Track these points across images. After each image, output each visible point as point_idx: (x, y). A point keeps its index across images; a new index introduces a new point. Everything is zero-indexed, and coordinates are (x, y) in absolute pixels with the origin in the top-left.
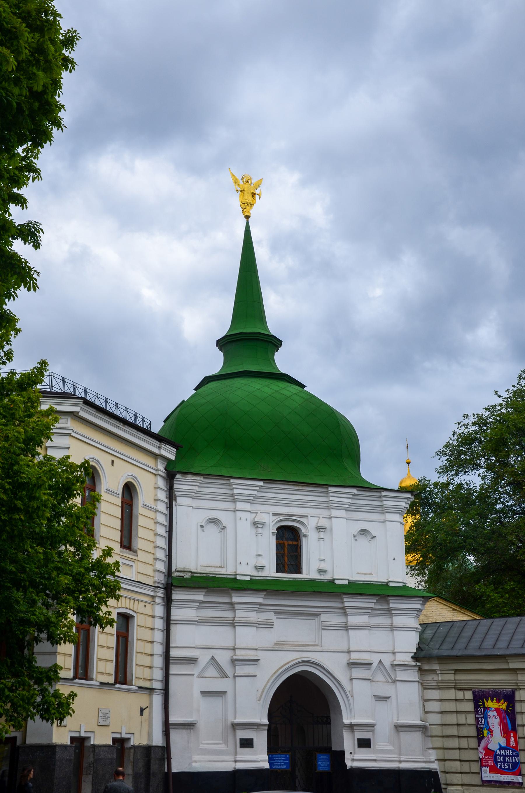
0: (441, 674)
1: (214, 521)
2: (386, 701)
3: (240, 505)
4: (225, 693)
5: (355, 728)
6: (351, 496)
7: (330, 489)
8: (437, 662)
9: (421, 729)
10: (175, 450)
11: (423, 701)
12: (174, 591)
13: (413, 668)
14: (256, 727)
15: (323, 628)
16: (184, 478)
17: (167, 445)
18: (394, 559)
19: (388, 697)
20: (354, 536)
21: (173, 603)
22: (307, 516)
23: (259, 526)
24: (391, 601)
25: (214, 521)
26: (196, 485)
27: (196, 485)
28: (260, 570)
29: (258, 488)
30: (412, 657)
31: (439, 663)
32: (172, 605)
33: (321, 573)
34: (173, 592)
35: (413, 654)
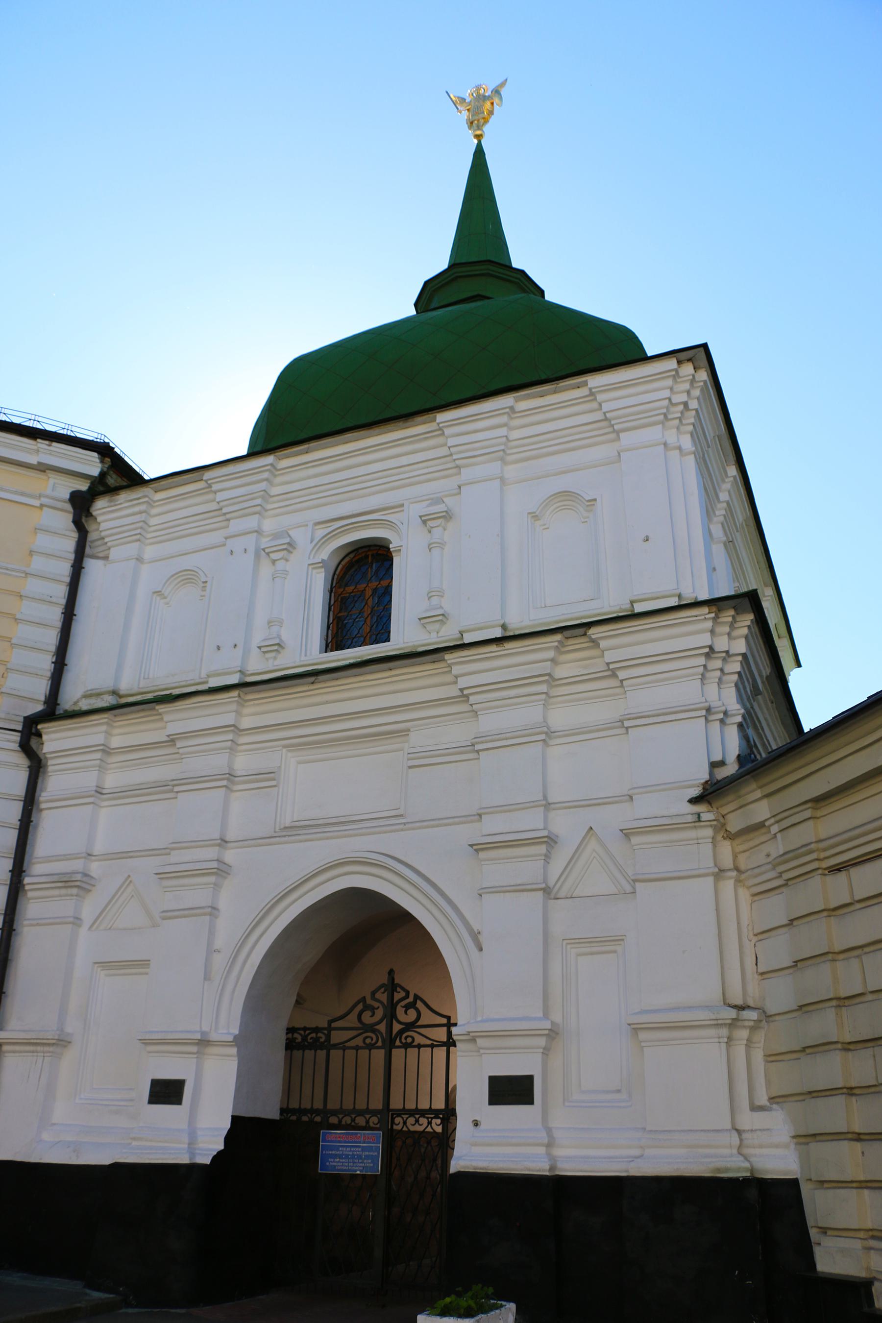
0: (780, 831)
1: (188, 577)
2: (615, 952)
3: (236, 525)
4: (144, 964)
5: (480, 1041)
6: (505, 419)
7: (442, 417)
8: (758, 794)
9: (724, 1032)
10: (96, 455)
11: (755, 939)
12: (47, 733)
13: (692, 834)
14: (194, 1049)
15: (411, 763)
16: (112, 504)
17: (54, 444)
18: (647, 539)
19: (619, 940)
20: (535, 517)
21: (50, 762)
22: (402, 505)
23: (274, 556)
24: (603, 644)
25: (188, 577)
26: (141, 512)
27: (141, 512)
28: (273, 654)
29: (265, 475)
30: (694, 801)
31: (767, 796)
32: (50, 769)
33: (429, 627)
34: (45, 737)
35: (695, 792)
